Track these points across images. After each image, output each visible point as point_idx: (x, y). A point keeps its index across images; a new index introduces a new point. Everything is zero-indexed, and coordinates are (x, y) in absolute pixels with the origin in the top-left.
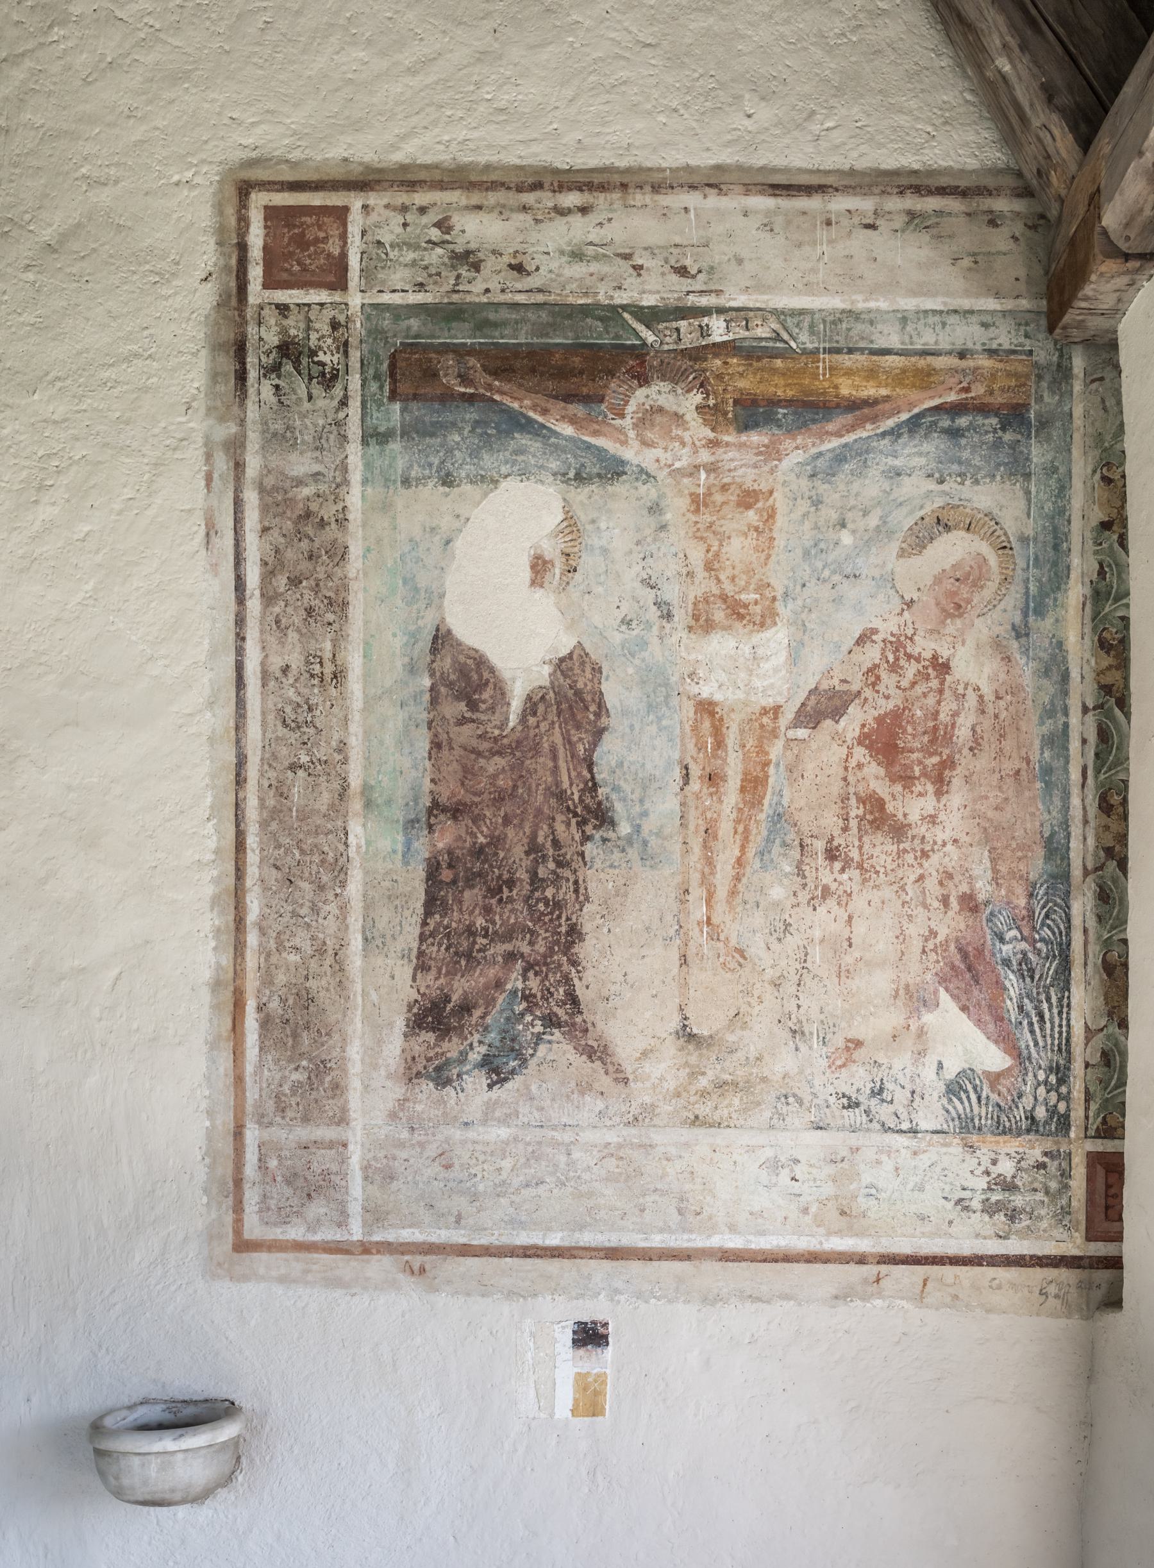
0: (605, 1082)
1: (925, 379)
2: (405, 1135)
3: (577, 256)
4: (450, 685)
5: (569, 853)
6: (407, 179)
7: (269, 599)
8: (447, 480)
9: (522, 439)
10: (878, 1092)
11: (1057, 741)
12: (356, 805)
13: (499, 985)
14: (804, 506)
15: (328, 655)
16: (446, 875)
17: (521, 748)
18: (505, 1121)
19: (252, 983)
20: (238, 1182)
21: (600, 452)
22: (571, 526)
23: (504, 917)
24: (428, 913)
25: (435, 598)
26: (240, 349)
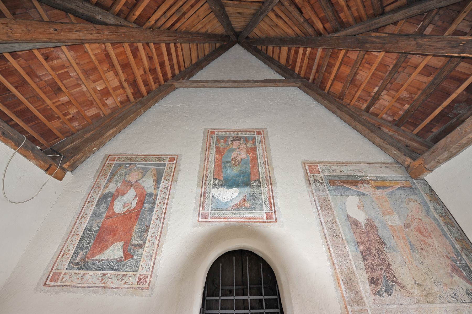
0: (408, 294)
1: (398, 183)
2: (377, 307)
3: (348, 170)
5: (382, 249)
6: (324, 163)
7: (322, 211)
8: (342, 196)
9: (349, 191)
10: (455, 294)
11: (443, 230)
12: (346, 243)
13: (381, 275)
16: (364, 254)
17: (367, 233)
18: (394, 303)
19: (339, 275)
21: (360, 192)
22: (361, 201)
23: (377, 261)
25: (346, 211)
26: (309, 180)
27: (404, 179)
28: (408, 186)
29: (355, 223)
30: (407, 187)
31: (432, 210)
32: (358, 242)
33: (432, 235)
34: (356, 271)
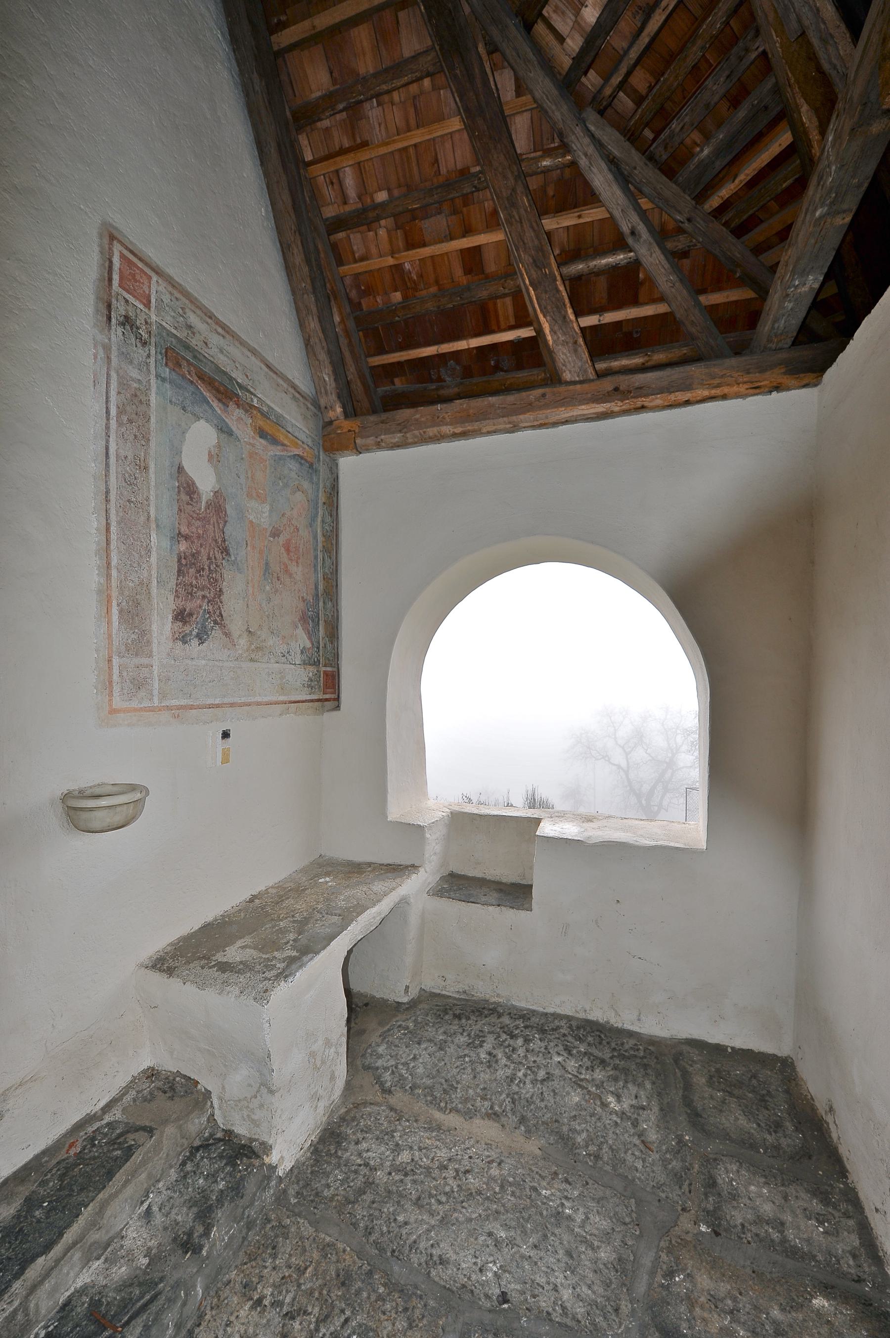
1: (296, 445)
2: (173, 662)
3: (221, 351)
4: (184, 488)
7: (120, 424)
8: (184, 409)
9: (205, 407)
10: (288, 652)
11: (316, 557)
12: (153, 526)
13: (200, 607)
14: (273, 470)
15: (142, 459)
16: (184, 562)
17: (204, 520)
19: (115, 593)
20: (111, 682)
21: (226, 424)
22: (219, 446)
23: (203, 581)
24: (179, 576)
25: (179, 453)
26: (109, 306)
27: (310, 443)
28: (309, 459)
29: (189, 489)
30: (306, 460)
31: (319, 519)
32: (180, 533)
33: (300, 561)
34: (154, 591)
